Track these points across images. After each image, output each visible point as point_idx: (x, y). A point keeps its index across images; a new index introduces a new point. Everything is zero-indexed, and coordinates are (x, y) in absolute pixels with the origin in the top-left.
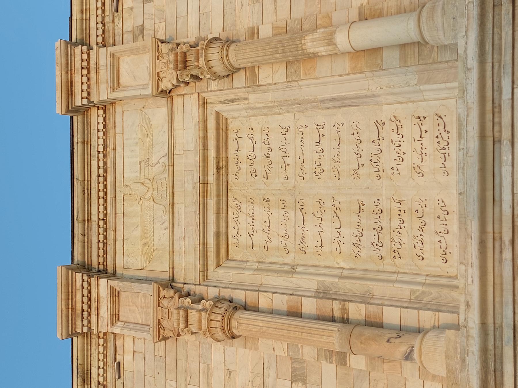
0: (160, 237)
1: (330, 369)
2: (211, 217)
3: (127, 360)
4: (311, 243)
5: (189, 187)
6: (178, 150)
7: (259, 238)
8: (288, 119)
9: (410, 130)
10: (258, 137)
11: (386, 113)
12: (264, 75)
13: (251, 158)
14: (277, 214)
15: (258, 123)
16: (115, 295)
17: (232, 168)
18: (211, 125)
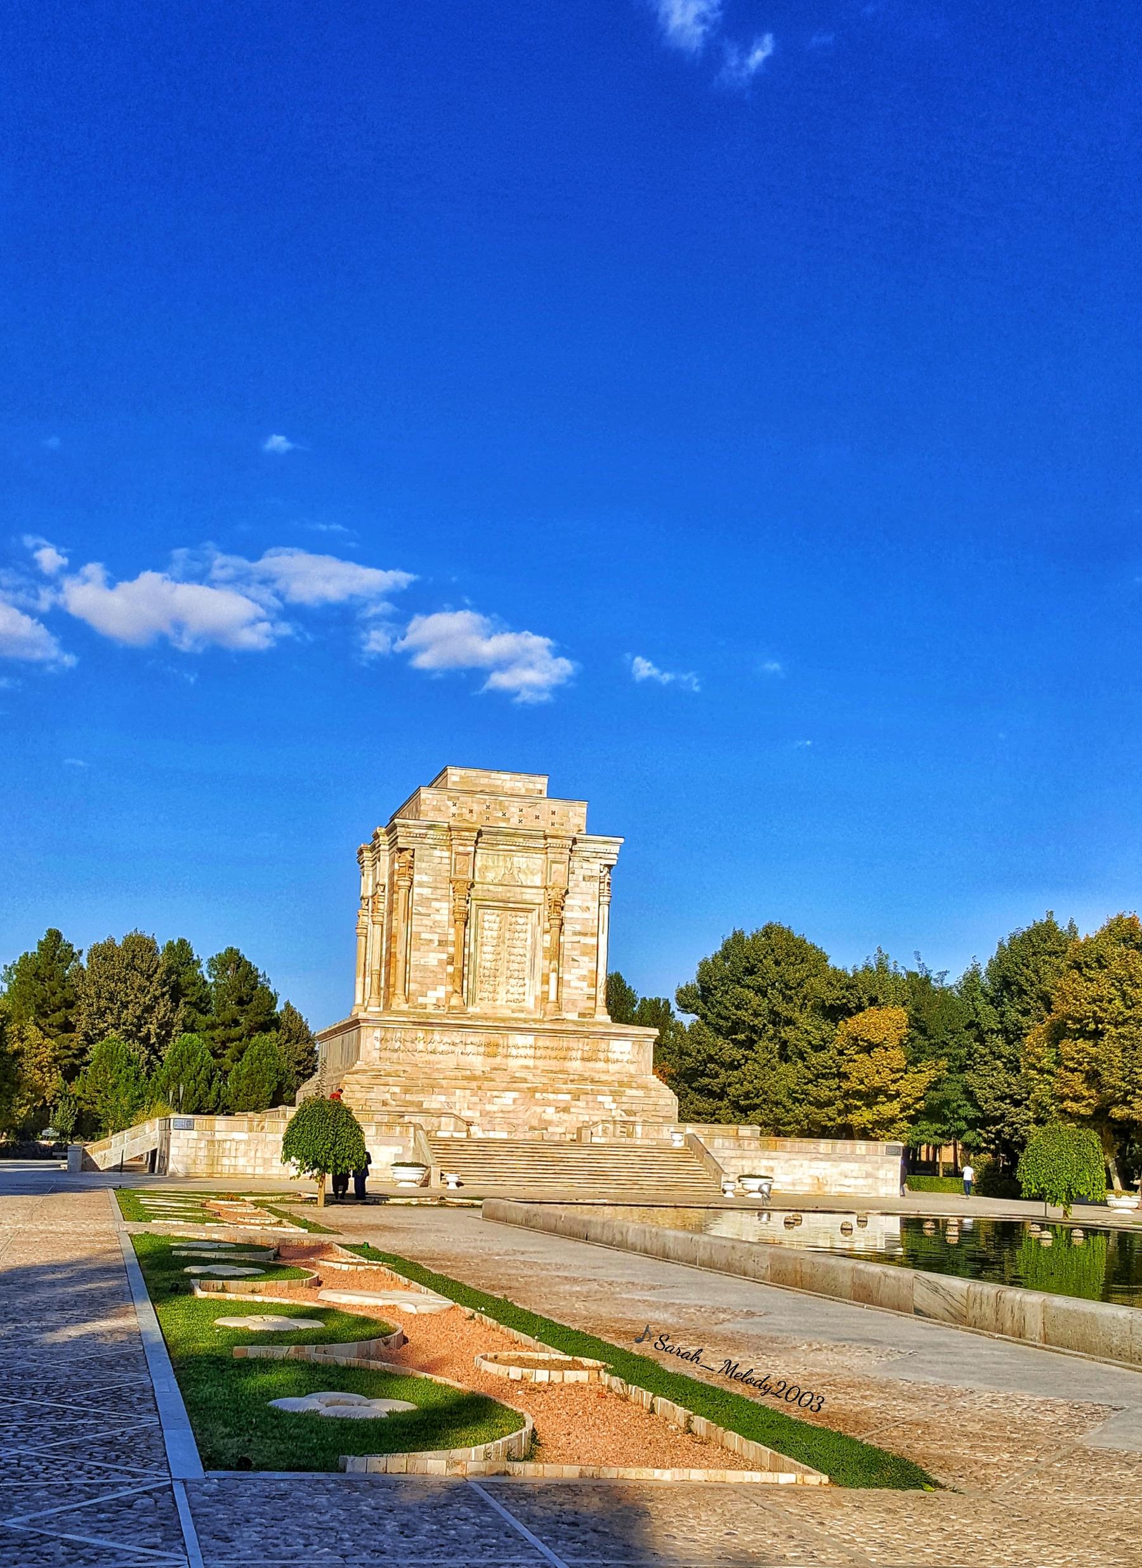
0: (490, 876)
1: (444, 956)
2: (496, 904)
3: (437, 853)
4: (485, 949)
5: (508, 895)
6: (524, 890)
7: (486, 925)
8: (529, 942)
9: (521, 990)
10: (524, 927)
11: (527, 981)
12: (547, 937)
13: (517, 923)
14: (495, 934)
15: (529, 927)
16: (468, 854)
17: (514, 913)
18: (531, 906)
